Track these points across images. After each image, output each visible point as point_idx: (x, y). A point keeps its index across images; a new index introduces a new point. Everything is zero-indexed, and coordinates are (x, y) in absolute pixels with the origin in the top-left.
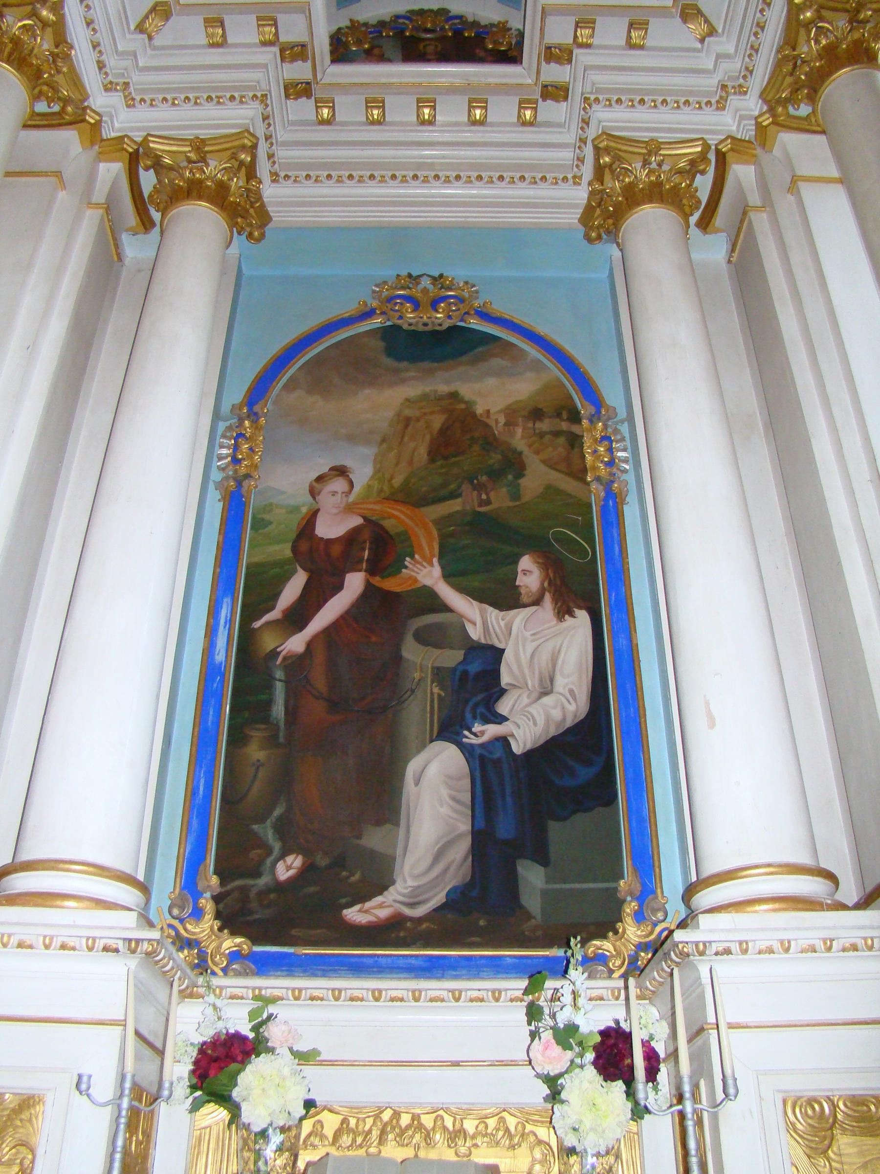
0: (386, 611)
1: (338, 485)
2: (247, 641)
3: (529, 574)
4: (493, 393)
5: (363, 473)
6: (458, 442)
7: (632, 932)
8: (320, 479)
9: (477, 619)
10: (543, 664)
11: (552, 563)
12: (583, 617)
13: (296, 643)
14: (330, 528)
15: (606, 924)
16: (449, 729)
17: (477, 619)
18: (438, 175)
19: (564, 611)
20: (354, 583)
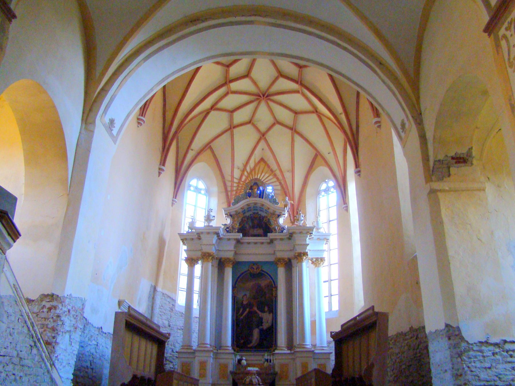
0: (251, 313)
1: (245, 297)
2: (237, 317)
3: (266, 309)
4: (263, 283)
5: (248, 295)
6: (259, 291)
7: (274, 348)
8: (244, 296)
9: (261, 314)
10: (267, 317)
11: (269, 308)
12: (271, 314)
13: (242, 317)
14: (245, 303)
15: (271, 347)
16: (258, 327)
17: (261, 314)
18: (253, 362)
19: (269, 313)
20: (248, 310)
